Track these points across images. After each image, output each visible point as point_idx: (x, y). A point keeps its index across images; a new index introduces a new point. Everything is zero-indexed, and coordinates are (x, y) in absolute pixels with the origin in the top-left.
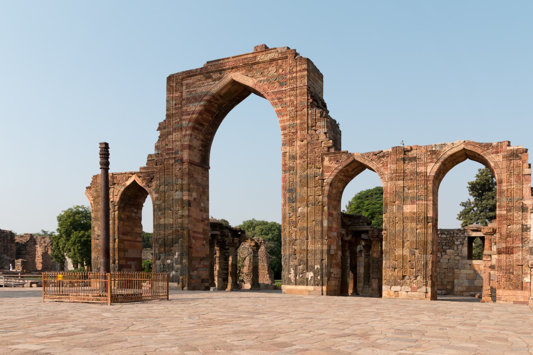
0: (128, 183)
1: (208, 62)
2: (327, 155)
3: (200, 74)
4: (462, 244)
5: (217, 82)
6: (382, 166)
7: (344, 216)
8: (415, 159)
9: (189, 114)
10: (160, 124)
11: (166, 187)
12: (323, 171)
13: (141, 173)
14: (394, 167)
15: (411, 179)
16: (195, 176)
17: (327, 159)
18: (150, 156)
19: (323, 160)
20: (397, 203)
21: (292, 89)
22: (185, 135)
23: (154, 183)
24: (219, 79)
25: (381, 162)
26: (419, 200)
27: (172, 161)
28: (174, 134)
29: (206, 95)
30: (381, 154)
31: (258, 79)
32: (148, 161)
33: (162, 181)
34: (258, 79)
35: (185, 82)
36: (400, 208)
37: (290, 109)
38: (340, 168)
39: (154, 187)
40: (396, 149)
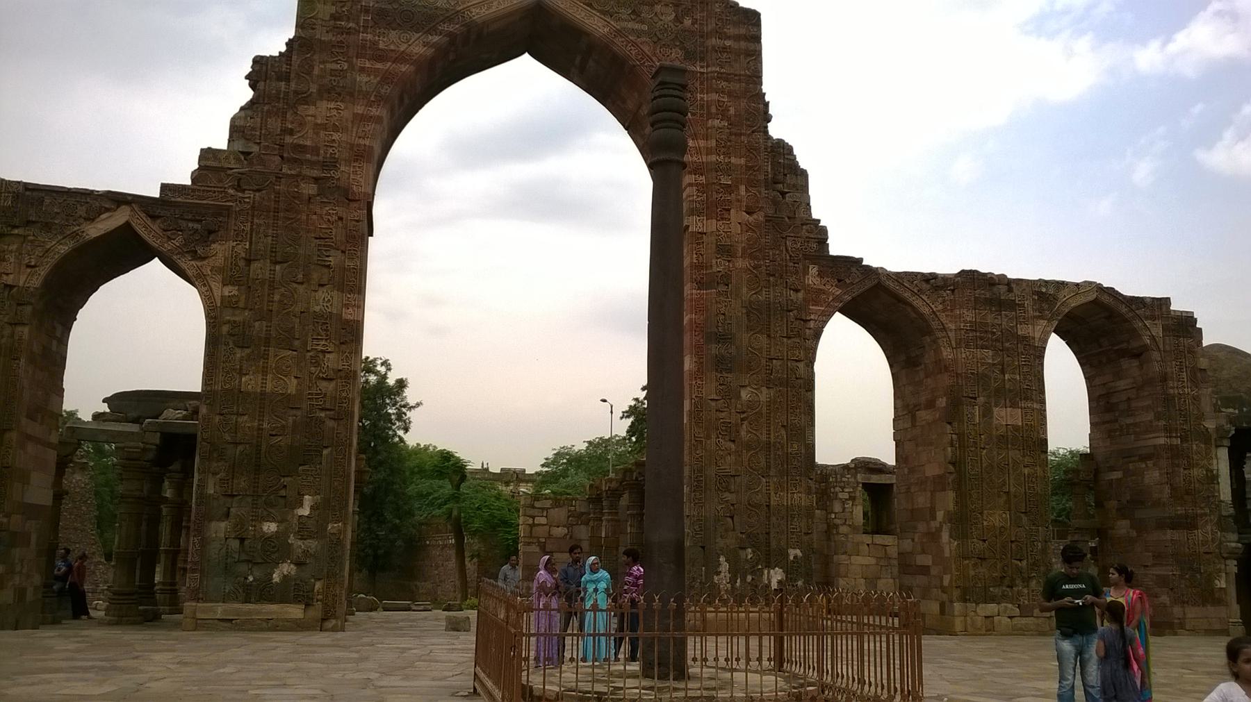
0: (95, 230)
6: (944, 310)
8: (1012, 305)
10: (259, 61)
11: (278, 267)
12: (804, 299)
14: (969, 315)
15: (1008, 349)
17: (813, 270)
19: (806, 272)
23: (220, 251)
25: (940, 300)
27: (309, 189)
28: (324, 105)
31: (624, 24)
34: (624, 24)
38: (848, 298)
39: (219, 261)
40: (970, 278)
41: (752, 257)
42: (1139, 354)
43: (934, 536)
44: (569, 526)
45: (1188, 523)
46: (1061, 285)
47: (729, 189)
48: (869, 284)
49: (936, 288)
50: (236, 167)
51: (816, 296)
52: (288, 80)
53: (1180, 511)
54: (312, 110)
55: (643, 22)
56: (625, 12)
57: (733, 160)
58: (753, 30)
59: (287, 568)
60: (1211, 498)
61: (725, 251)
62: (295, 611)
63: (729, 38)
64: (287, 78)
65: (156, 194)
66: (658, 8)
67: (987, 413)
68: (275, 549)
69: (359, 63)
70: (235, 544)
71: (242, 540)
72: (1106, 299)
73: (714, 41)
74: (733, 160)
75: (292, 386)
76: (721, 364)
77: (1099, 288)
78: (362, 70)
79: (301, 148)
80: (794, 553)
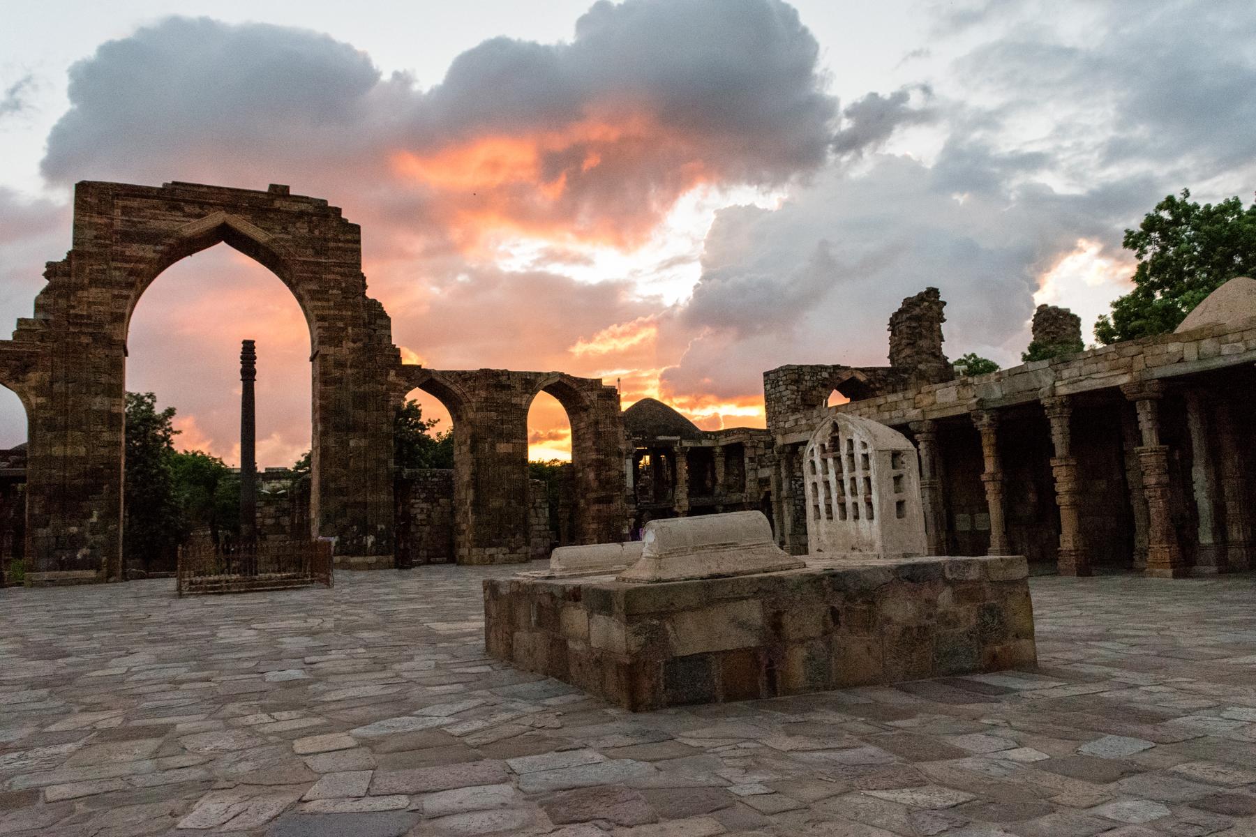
1: (174, 183)
3: (154, 197)
5: (193, 221)
8: (509, 387)
9: (127, 262)
10: (49, 265)
14: (483, 394)
17: (392, 373)
18: (21, 321)
19: (388, 374)
23: (34, 377)
24: (199, 216)
27: (85, 340)
28: (93, 290)
30: (467, 376)
32: (19, 330)
33: (60, 373)
35: (121, 203)
39: (33, 384)
40: (486, 373)
42: (586, 409)
43: (466, 513)
44: (276, 518)
45: (608, 500)
46: (540, 374)
47: (343, 329)
48: (425, 379)
50: (41, 330)
52: (70, 276)
53: (603, 494)
54: (86, 294)
55: (288, 233)
56: (278, 228)
58: (356, 237)
59: (85, 551)
60: (621, 487)
61: (340, 365)
62: (92, 574)
63: (340, 241)
64: (68, 275)
66: (298, 225)
67: (493, 446)
68: (75, 542)
69: (114, 264)
70: (53, 540)
71: (57, 538)
72: (565, 381)
73: (332, 244)
75: (82, 451)
76: (337, 428)
77: (562, 375)
78: (115, 268)
80: (381, 527)
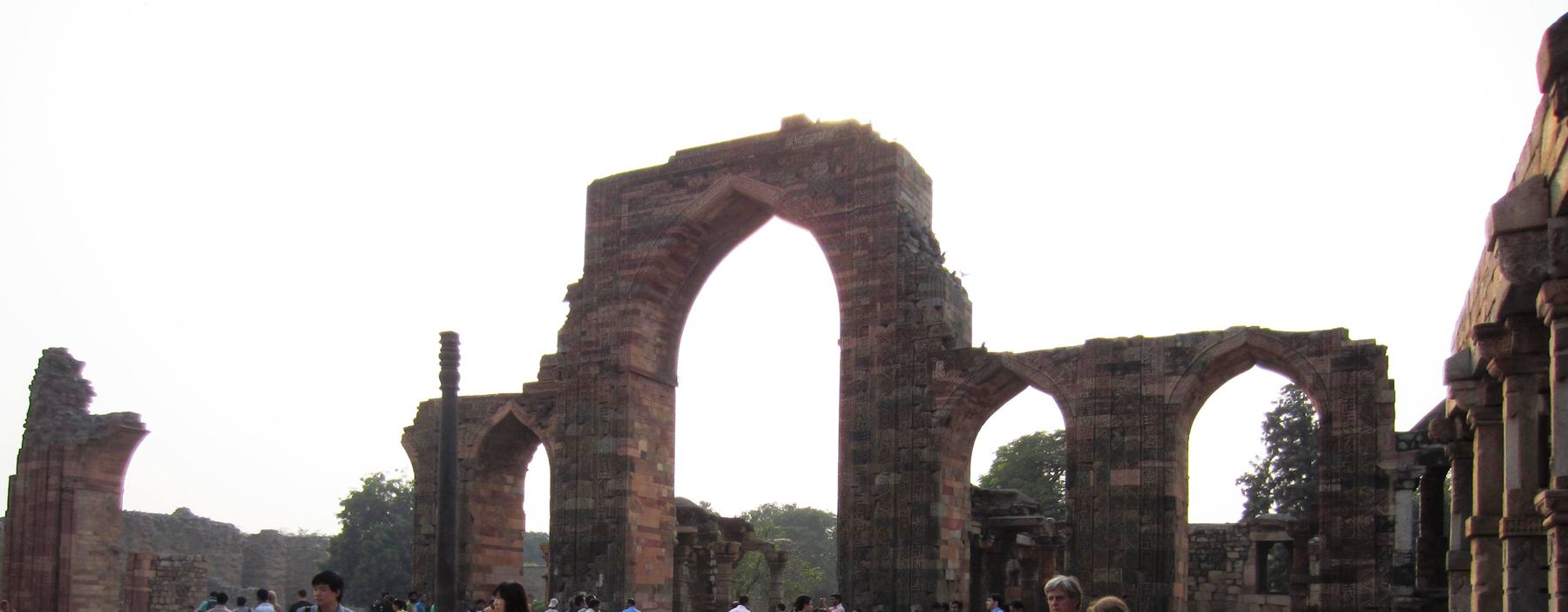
0: (497, 418)
2: (940, 356)
4: (1244, 558)
5: (696, 196)
6: (1066, 381)
7: (976, 492)
8: (1137, 366)
10: (571, 288)
13: (525, 395)
14: (1090, 383)
15: (1128, 412)
16: (646, 403)
17: (940, 365)
19: (931, 367)
20: (1097, 464)
21: (865, 211)
22: (624, 313)
26: (1147, 458)
28: (601, 309)
29: (672, 224)
30: (1061, 357)
36: (1103, 476)
37: (859, 253)
39: (553, 428)
41: (885, 363)
49: (1058, 363)
51: (941, 388)
57: (871, 282)
64: (580, 297)
65: (520, 391)
66: (815, 166)
74: (871, 282)
79: (589, 343)
